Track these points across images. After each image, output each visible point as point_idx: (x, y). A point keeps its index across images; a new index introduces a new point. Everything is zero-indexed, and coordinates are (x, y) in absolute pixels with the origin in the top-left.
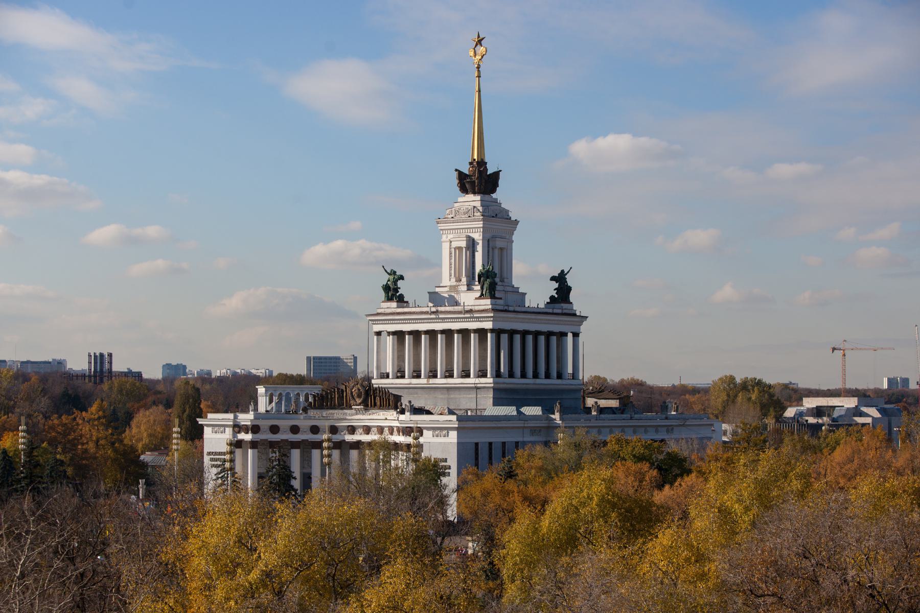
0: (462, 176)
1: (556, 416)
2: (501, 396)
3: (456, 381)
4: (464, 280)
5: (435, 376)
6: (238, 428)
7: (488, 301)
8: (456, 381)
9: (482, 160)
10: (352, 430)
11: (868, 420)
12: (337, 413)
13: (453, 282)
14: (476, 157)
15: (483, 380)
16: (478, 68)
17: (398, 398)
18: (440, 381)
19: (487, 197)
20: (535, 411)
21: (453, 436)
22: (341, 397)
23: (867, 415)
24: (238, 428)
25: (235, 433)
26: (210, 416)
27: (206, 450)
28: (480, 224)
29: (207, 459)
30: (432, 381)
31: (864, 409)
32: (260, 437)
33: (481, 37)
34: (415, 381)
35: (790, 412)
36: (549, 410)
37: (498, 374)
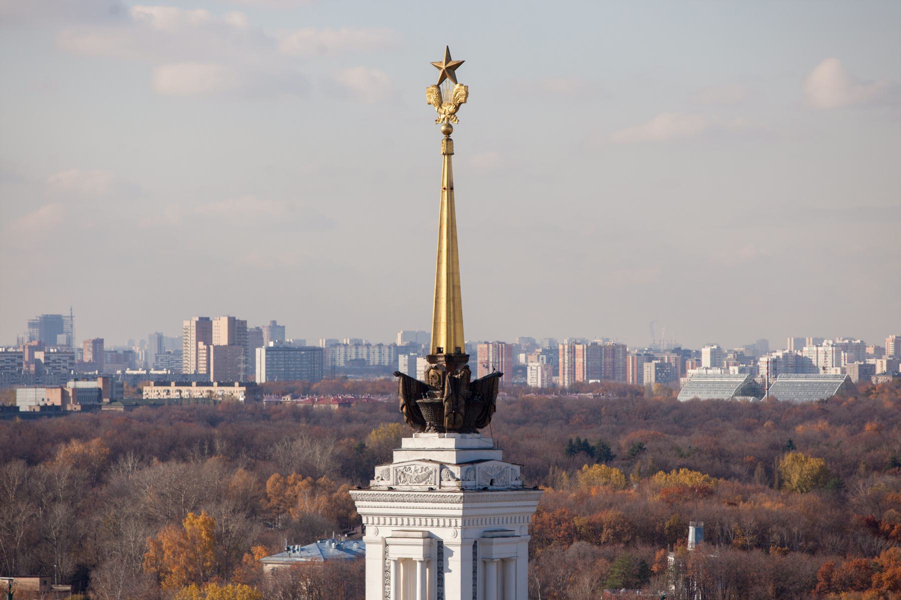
9: (458, 349)
14: (443, 344)
16: (448, 133)
19: (472, 440)
28: (457, 509)
33: (455, 59)
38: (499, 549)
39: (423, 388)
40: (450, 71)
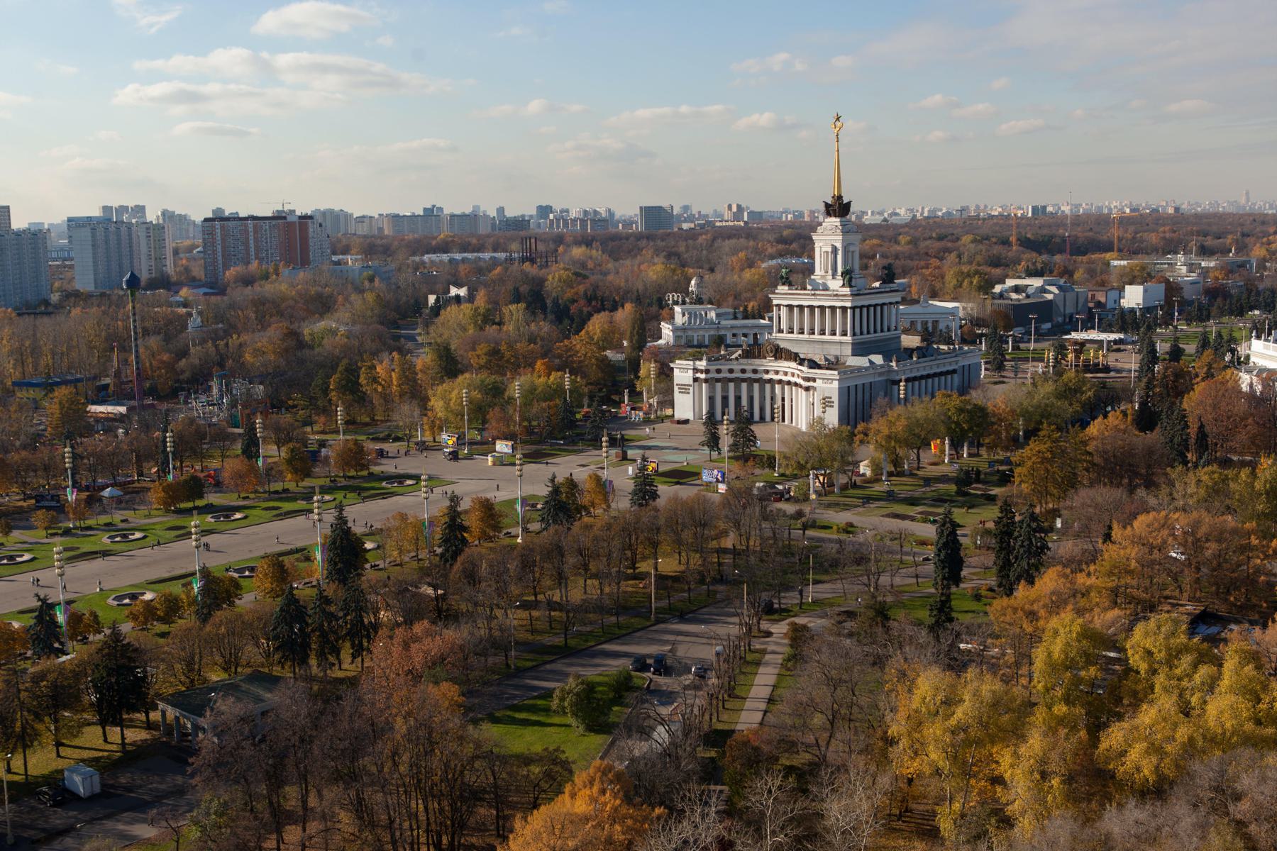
0: (827, 206)
1: (894, 364)
2: (860, 349)
3: (827, 337)
4: (830, 272)
5: (813, 333)
6: (696, 370)
7: (848, 289)
8: (827, 337)
10: (767, 372)
11: (1050, 297)
12: (757, 361)
13: (823, 273)
15: (845, 338)
17: (796, 355)
18: (816, 337)
19: (844, 219)
20: (878, 359)
21: (836, 384)
22: (759, 352)
23: (1050, 292)
24: (696, 370)
25: (694, 373)
26: (677, 362)
27: (675, 382)
28: (841, 238)
29: (676, 388)
30: (812, 336)
31: (1048, 287)
32: (710, 376)
34: (801, 336)
35: (998, 289)
36: (888, 358)
37: (854, 334)
38: (852, 248)
39: (831, 205)
40: (838, 119)
